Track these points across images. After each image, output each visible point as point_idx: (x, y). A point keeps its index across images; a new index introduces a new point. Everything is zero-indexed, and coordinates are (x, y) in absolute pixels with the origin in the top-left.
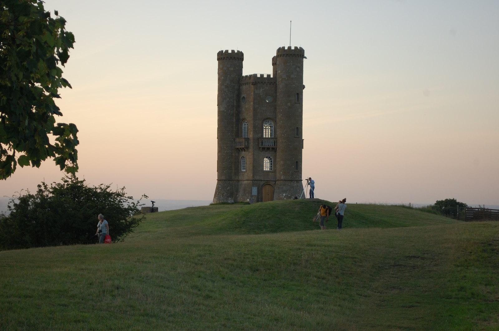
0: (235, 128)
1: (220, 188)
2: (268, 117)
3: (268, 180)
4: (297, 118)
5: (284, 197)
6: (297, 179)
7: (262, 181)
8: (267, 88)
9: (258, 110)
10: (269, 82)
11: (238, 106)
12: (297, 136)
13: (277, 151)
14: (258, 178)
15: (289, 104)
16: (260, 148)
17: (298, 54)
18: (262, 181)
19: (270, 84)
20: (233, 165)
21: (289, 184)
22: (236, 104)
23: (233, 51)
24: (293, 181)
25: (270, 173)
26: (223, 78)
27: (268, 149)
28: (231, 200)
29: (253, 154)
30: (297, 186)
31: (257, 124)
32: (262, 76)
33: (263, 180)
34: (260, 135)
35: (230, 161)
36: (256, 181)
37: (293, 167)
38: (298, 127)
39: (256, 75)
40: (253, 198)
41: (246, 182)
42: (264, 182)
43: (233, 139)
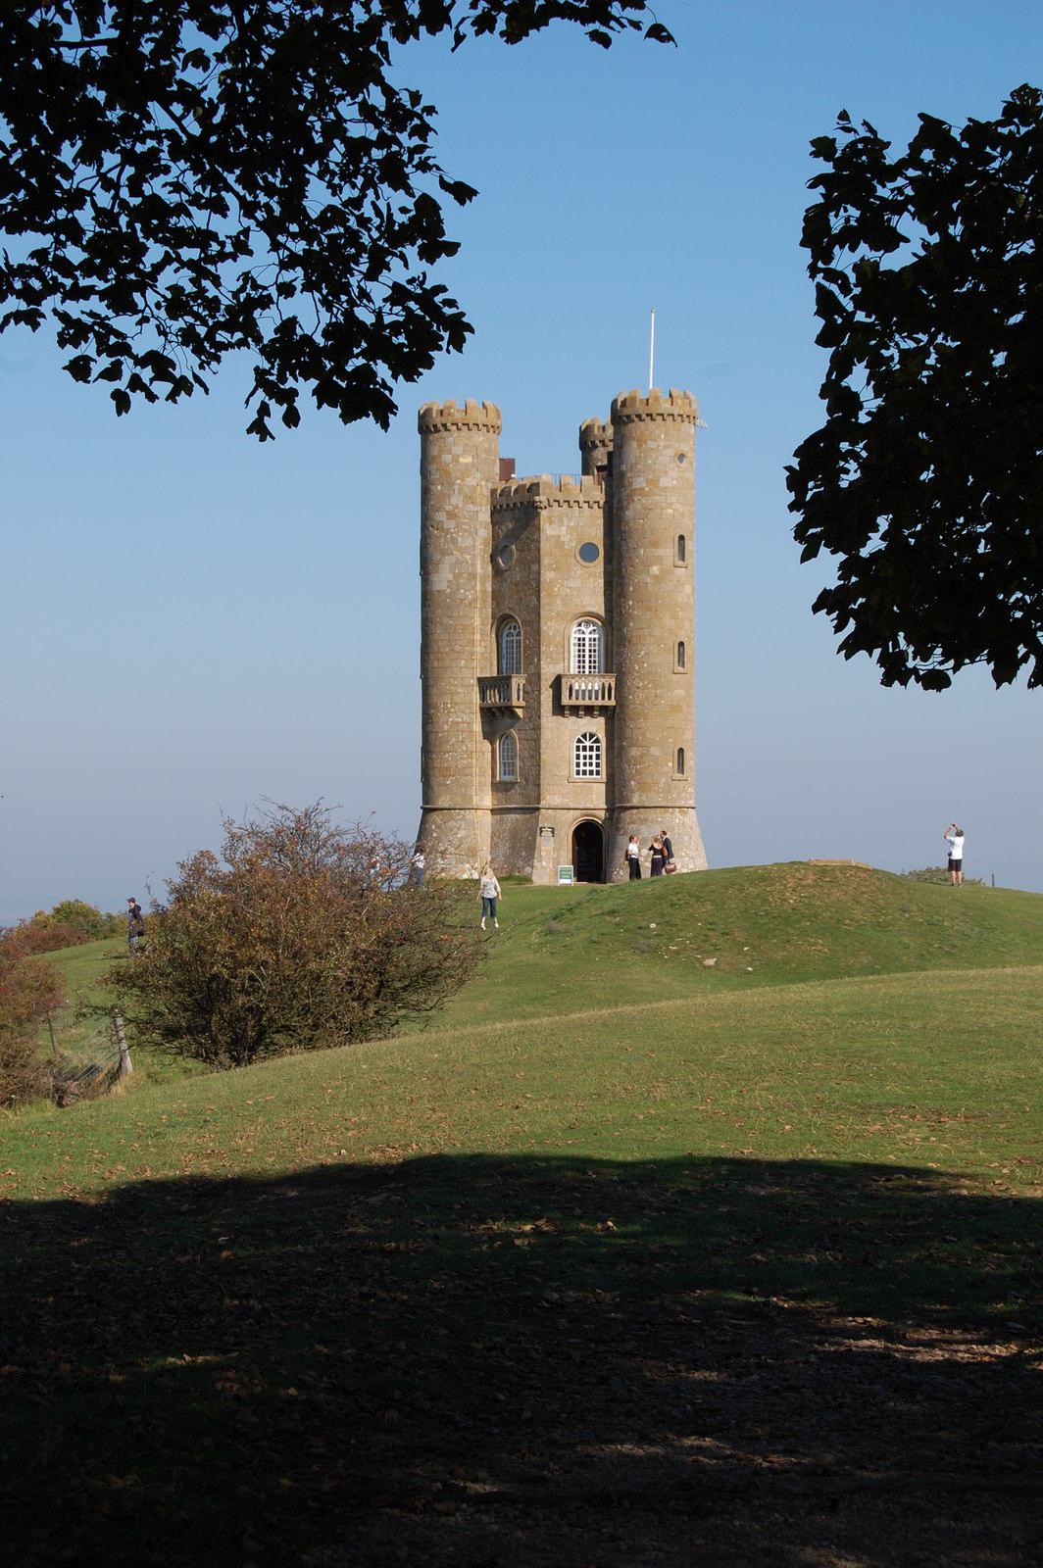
1: (435, 835)
2: (589, 609)
3: (588, 806)
6: (682, 804)
10: (588, 502)
14: (557, 801)
17: (682, 413)
26: (439, 487)
33: (572, 806)
35: (465, 749)
37: (670, 764)
40: (544, 864)
43: (473, 678)
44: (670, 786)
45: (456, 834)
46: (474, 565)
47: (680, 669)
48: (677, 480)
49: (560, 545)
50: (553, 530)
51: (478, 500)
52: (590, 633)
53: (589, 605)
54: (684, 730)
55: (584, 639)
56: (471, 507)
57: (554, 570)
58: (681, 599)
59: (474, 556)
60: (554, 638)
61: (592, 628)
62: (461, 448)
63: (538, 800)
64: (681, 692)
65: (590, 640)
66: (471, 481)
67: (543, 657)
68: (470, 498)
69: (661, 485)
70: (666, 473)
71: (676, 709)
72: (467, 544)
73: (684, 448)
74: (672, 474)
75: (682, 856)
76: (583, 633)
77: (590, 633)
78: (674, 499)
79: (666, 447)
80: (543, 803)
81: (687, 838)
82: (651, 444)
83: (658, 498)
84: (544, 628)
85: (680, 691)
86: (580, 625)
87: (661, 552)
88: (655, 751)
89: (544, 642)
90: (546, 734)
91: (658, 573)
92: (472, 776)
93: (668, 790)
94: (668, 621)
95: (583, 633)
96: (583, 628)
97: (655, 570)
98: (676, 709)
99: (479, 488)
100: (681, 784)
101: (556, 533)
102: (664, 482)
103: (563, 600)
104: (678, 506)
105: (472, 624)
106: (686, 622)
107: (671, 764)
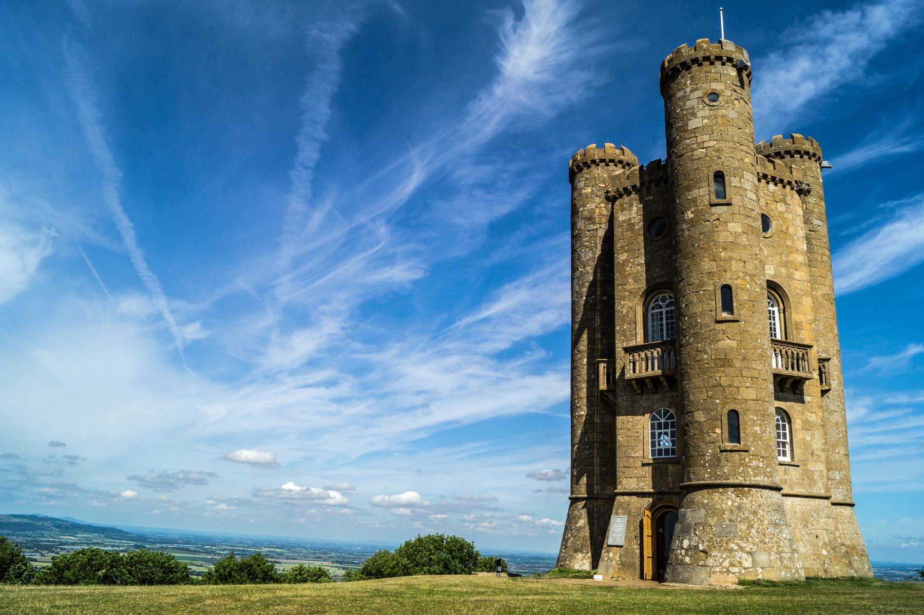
0: (601, 343)
4: (723, 254)
5: (683, 552)
6: (740, 480)
8: (651, 198)
9: (628, 269)
17: (708, 54)
19: (657, 185)
20: (596, 451)
21: (706, 501)
22: (601, 275)
24: (721, 490)
25: (670, 467)
28: (582, 560)
30: (739, 508)
31: (625, 311)
35: (587, 440)
36: (626, 497)
37: (718, 431)
38: (728, 282)
40: (611, 555)
44: (719, 460)
45: (577, 523)
47: (725, 315)
48: (708, 118)
50: (625, 215)
51: (597, 220)
52: (667, 306)
53: (658, 277)
54: (738, 388)
55: (661, 313)
56: (592, 227)
57: (626, 251)
58: (722, 237)
60: (628, 316)
61: (667, 301)
62: (583, 183)
63: (614, 483)
64: (727, 343)
65: (667, 312)
66: (590, 206)
67: (617, 336)
68: (590, 219)
69: (689, 128)
70: (694, 115)
71: (725, 361)
72: (588, 257)
73: (717, 86)
75: (731, 550)
76: (661, 307)
77: (667, 306)
78: (706, 138)
79: (692, 91)
80: (619, 489)
81: (743, 527)
82: (680, 94)
83: (688, 141)
84: (618, 307)
85: (728, 341)
86: (657, 300)
87: (695, 193)
88: (700, 416)
89: (617, 322)
91: (692, 216)
92: (593, 466)
93: (716, 463)
94: (707, 265)
95: (661, 307)
96: (660, 303)
97: (690, 215)
98: (725, 361)
99: (597, 211)
100: (736, 456)
101: (628, 217)
102: (693, 124)
103: (634, 278)
104: (712, 143)
105: (593, 325)
106: (732, 262)
107: (720, 432)
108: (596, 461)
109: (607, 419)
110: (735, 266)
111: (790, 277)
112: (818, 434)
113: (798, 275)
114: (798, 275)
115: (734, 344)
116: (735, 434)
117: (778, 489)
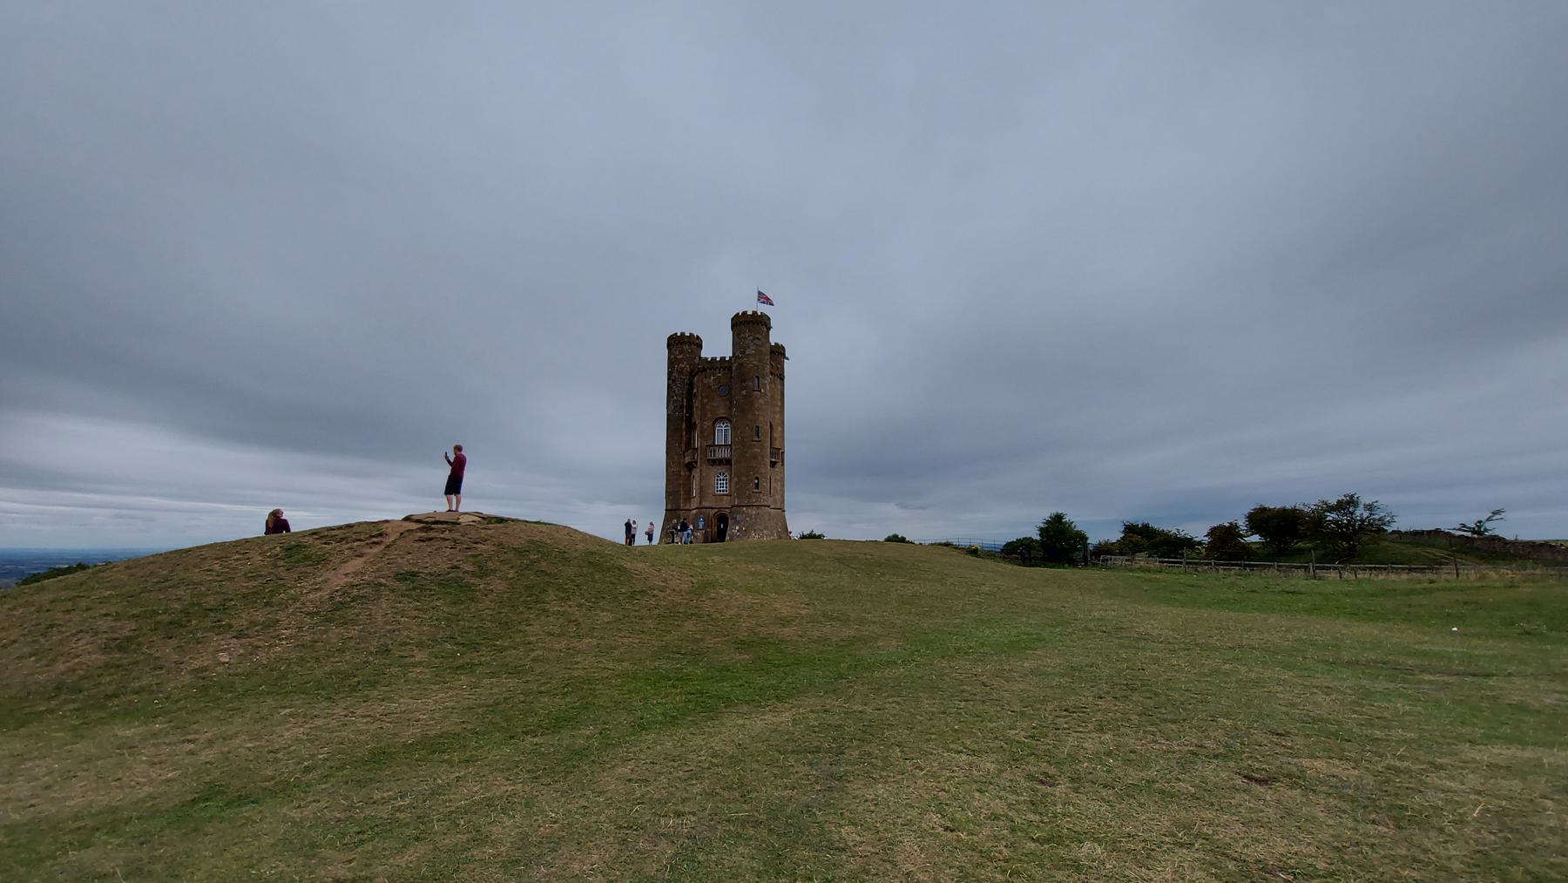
7: (713, 508)
11: (690, 407)
12: (757, 439)
13: (733, 463)
14: (706, 504)
15: (744, 392)
16: (709, 460)
18: (713, 508)
19: (724, 370)
23: (683, 334)
27: (720, 462)
29: (701, 471)
32: (714, 359)
34: (710, 443)
39: (707, 359)
41: (694, 511)
42: (716, 510)
46: (683, 401)
49: (710, 387)
59: (683, 399)
74: (752, 348)
90: (704, 474)
108: (682, 492)
109: (687, 473)
110: (761, 418)
111: (774, 417)
112: (779, 483)
113: (777, 417)
114: (777, 417)
115: (759, 450)
116: (757, 486)
117: (769, 506)
